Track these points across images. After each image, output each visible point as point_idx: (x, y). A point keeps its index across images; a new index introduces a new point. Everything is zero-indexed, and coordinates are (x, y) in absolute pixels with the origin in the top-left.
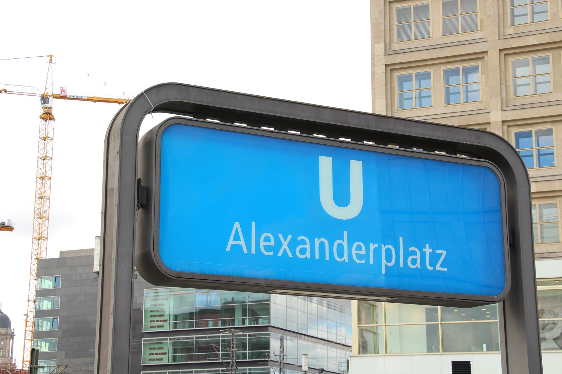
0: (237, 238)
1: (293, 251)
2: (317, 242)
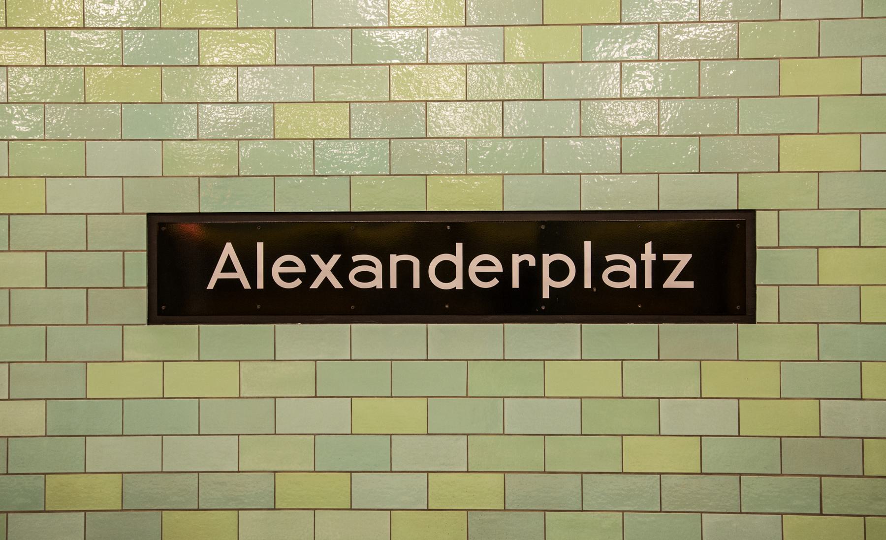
0: (229, 267)
1: (344, 279)
2: (394, 259)
